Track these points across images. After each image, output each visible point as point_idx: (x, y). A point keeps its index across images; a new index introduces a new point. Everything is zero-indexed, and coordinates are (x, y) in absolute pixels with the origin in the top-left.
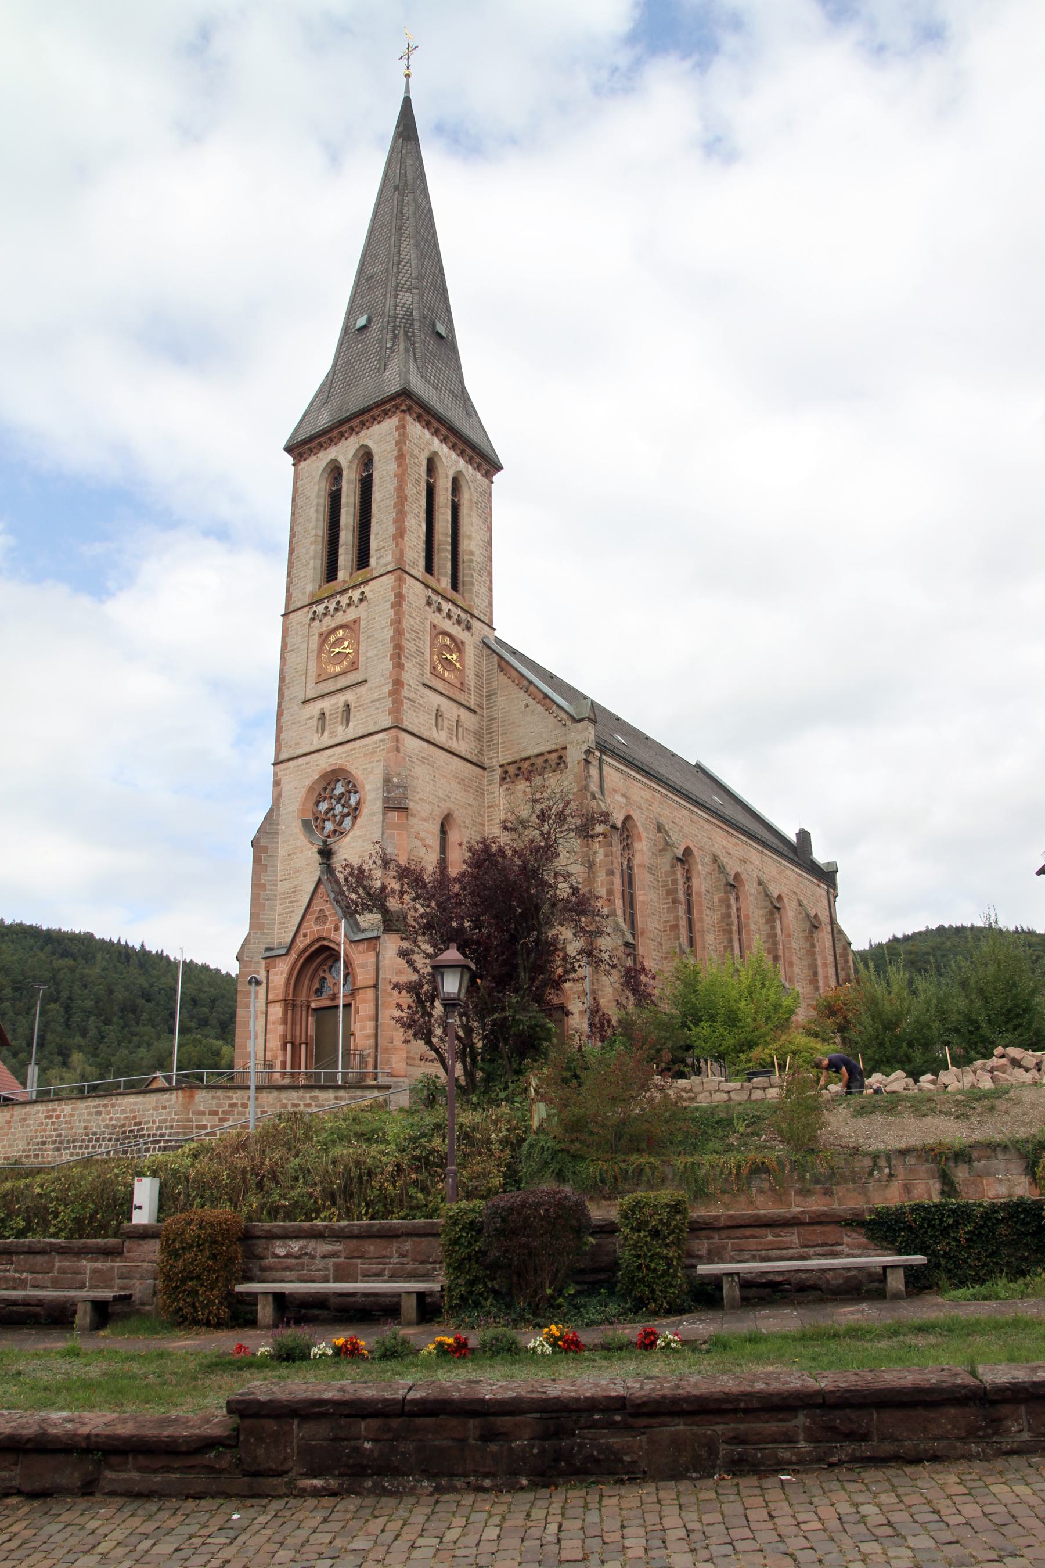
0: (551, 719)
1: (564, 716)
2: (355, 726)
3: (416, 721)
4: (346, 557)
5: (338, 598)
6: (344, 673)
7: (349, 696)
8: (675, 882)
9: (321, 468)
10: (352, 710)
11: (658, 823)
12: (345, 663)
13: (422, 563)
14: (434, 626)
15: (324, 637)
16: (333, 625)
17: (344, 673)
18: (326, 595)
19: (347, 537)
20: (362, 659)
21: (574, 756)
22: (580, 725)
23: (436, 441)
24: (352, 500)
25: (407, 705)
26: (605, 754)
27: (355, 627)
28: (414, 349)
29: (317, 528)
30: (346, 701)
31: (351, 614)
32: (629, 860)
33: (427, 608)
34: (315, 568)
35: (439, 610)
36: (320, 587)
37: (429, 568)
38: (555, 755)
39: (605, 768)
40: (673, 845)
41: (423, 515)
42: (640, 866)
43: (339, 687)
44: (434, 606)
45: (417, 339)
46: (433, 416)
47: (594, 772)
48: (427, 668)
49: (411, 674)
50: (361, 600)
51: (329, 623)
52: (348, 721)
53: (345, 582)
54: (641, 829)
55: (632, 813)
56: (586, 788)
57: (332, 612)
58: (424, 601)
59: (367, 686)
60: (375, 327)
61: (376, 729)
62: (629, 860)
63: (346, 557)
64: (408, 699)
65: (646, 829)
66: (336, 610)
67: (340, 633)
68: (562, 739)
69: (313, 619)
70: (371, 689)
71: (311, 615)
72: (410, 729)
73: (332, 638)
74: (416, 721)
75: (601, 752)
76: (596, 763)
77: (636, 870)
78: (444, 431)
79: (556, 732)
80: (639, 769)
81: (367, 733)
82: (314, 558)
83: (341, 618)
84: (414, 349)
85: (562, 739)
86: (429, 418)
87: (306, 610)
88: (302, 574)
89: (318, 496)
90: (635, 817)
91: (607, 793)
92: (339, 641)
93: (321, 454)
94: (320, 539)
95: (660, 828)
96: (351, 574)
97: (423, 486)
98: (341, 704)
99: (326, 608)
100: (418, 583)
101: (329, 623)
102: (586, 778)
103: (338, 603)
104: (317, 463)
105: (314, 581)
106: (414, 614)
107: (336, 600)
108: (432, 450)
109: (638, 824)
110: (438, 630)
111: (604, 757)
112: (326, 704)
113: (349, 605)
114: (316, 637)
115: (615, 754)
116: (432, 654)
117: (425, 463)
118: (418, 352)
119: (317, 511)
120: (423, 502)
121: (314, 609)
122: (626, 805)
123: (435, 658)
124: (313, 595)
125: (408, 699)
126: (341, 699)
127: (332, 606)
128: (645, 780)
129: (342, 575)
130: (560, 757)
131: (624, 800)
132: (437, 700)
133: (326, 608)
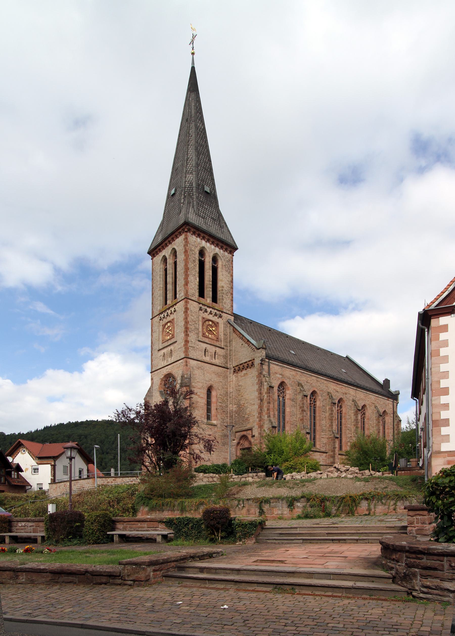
0: (250, 349)
1: (254, 348)
2: (174, 358)
3: (195, 354)
4: (170, 295)
5: (167, 311)
6: (170, 339)
7: (172, 347)
8: (303, 404)
9: (160, 260)
10: (173, 352)
11: (298, 383)
12: (171, 335)
13: (197, 294)
14: (204, 318)
15: (164, 326)
16: (167, 322)
17: (170, 339)
18: (164, 310)
19: (170, 287)
20: (175, 333)
21: (257, 362)
22: (259, 350)
23: (203, 242)
24: (171, 272)
25: (190, 349)
26: (271, 360)
27: (173, 322)
28: (193, 202)
29: (160, 284)
30: (171, 349)
31: (172, 317)
32: (283, 397)
33: (201, 312)
34: (160, 300)
35: (206, 311)
36: (163, 307)
37: (202, 294)
38: (251, 362)
39: (272, 366)
40: (304, 391)
41: (197, 275)
42: (288, 399)
43: (169, 344)
44: (203, 311)
45: (195, 197)
46: (201, 231)
47: (265, 367)
48: (201, 334)
49: (192, 337)
50: (175, 311)
51: (165, 321)
52: (172, 356)
53: (169, 304)
54: (289, 386)
55: (284, 380)
56: (261, 373)
57: (166, 317)
58: (198, 309)
59: (177, 343)
60: (177, 194)
61: (180, 358)
62: (283, 397)
63: (170, 295)
64: (191, 347)
65: (292, 386)
66: (167, 316)
67: (169, 324)
68: (253, 356)
69: (160, 320)
70: (178, 344)
71: (159, 318)
72: (192, 358)
73: (167, 326)
74: (195, 354)
75: (269, 360)
76: (267, 364)
77: (286, 400)
78: (207, 237)
79: (251, 354)
80: (289, 364)
81: (177, 360)
82: (160, 296)
83: (169, 319)
84: (193, 202)
85: (253, 356)
86: (199, 232)
87: (158, 316)
88: (156, 303)
89: (160, 271)
90: (286, 382)
91: (271, 374)
92: (169, 327)
93: (160, 254)
94: (162, 288)
95: (299, 384)
96: (172, 301)
97: (197, 262)
98: (169, 350)
99: (164, 315)
100: (195, 303)
101: (165, 321)
102: (261, 370)
103: (167, 313)
104: (159, 258)
105: (160, 305)
106: (194, 315)
107: (167, 312)
108: (201, 246)
109: (287, 384)
110: (205, 319)
111: (270, 361)
112: (165, 351)
113: (171, 313)
114: (161, 326)
115: (277, 360)
116: (203, 329)
117: (198, 252)
118: (195, 203)
119: (160, 277)
120: (197, 269)
121: (160, 316)
122: (282, 378)
123: (205, 330)
124: (160, 310)
125: (191, 347)
126: (169, 348)
127: (166, 314)
128: (292, 368)
129: (169, 302)
130: (252, 363)
131: (281, 376)
132: (205, 346)
133: (164, 315)
